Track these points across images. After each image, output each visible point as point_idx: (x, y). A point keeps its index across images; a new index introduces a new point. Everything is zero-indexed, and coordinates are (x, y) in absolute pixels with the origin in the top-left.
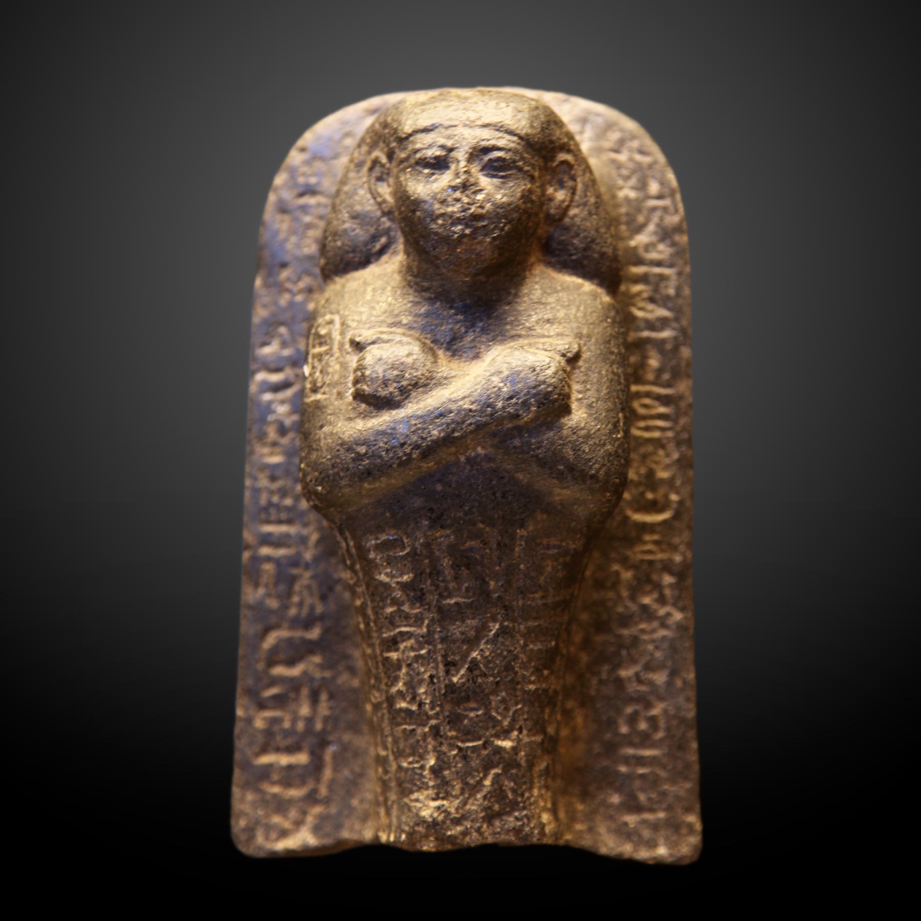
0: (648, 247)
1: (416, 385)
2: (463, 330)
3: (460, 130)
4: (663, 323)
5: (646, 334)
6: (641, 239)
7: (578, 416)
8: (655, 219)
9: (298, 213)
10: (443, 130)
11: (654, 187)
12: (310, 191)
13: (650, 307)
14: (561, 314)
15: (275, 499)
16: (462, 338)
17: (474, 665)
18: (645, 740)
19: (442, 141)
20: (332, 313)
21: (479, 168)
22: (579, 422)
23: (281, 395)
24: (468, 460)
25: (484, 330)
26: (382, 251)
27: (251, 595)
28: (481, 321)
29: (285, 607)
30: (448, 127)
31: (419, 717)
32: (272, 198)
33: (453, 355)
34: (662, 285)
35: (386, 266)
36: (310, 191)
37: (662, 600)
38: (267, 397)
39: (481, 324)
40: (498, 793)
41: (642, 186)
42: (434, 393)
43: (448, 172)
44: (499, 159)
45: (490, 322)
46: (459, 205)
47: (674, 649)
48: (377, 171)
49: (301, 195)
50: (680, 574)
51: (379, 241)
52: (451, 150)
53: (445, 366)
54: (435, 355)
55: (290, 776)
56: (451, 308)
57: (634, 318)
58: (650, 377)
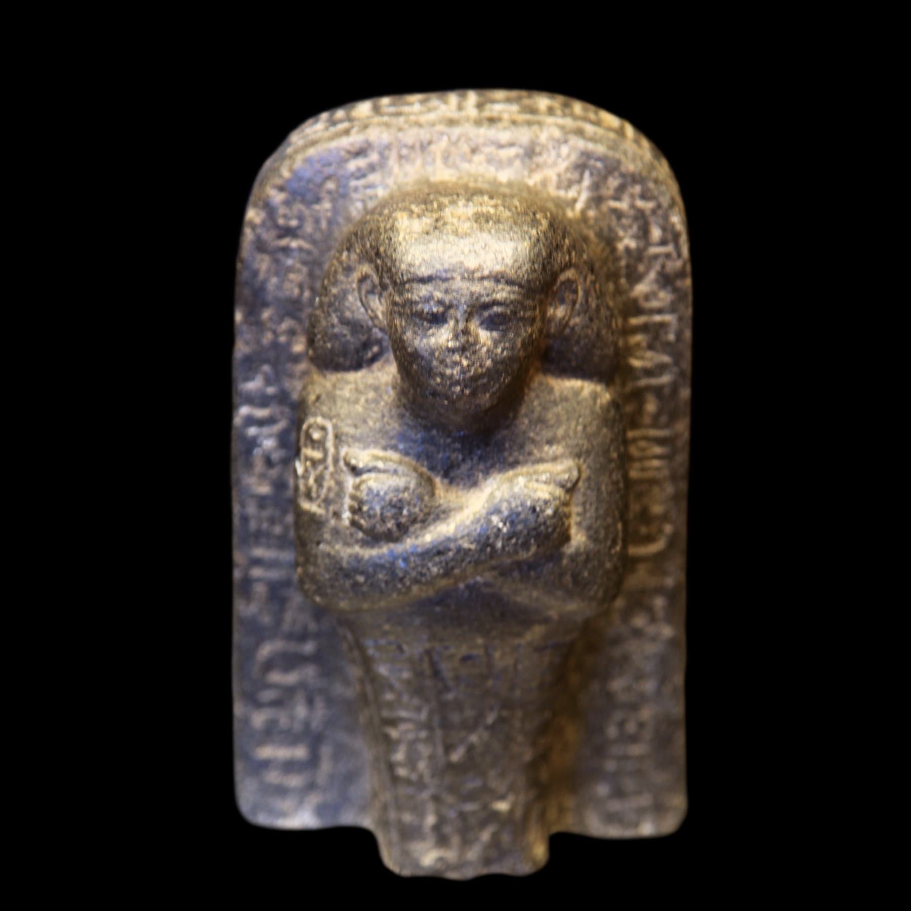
0: (647, 297)
1: (414, 521)
2: (460, 457)
3: (458, 284)
4: (661, 369)
5: (643, 382)
6: (641, 288)
7: (578, 539)
8: (657, 267)
9: (281, 256)
10: (440, 283)
11: (656, 233)
12: (288, 232)
13: (649, 354)
14: (560, 432)
15: (265, 525)
16: (459, 466)
17: (471, 749)
18: (634, 739)
19: (438, 295)
20: (324, 416)
21: (478, 323)
22: (578, 549)
23: (266, 430)
24: (468, 587)
25: (481, 459)
26: (374, 359)
27: (243, 609)
28: (479, 448)
29: (278, 621)
30: (446, 280)
31: (420, 785)
32: (248, 234)
33: (451, 482)
34: (662, 332)
35: (379, 374)
36: (288, 232)
37: (653, 620)
38: (252, 431)
39: (479, 452)
40: (495, 842)
41: (644, 233)
42: (432, 528)
43: (446, 326)
44: (498, 315)
45: (488, 449)
46: (458, 368)
47: (663, 661)
48: (367, 286)
49: (280, 237)
50: (671, 596)
51: (371, 348)
52: (450, 306)
53: (445, 494)
54: (430, 481)
55: (289, 766)
56: (449, 436)
57: (631, 369)
58: (647, 420)
